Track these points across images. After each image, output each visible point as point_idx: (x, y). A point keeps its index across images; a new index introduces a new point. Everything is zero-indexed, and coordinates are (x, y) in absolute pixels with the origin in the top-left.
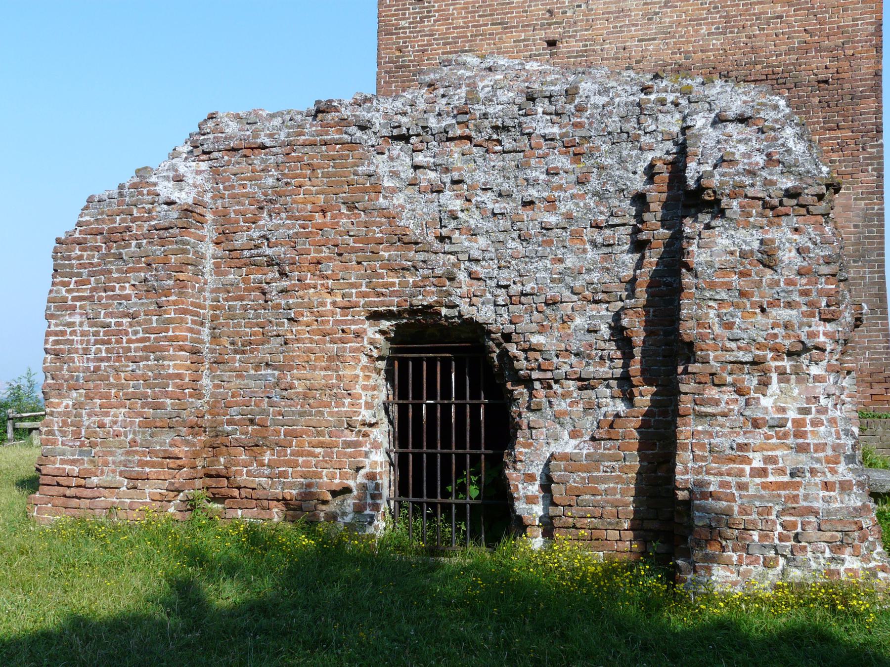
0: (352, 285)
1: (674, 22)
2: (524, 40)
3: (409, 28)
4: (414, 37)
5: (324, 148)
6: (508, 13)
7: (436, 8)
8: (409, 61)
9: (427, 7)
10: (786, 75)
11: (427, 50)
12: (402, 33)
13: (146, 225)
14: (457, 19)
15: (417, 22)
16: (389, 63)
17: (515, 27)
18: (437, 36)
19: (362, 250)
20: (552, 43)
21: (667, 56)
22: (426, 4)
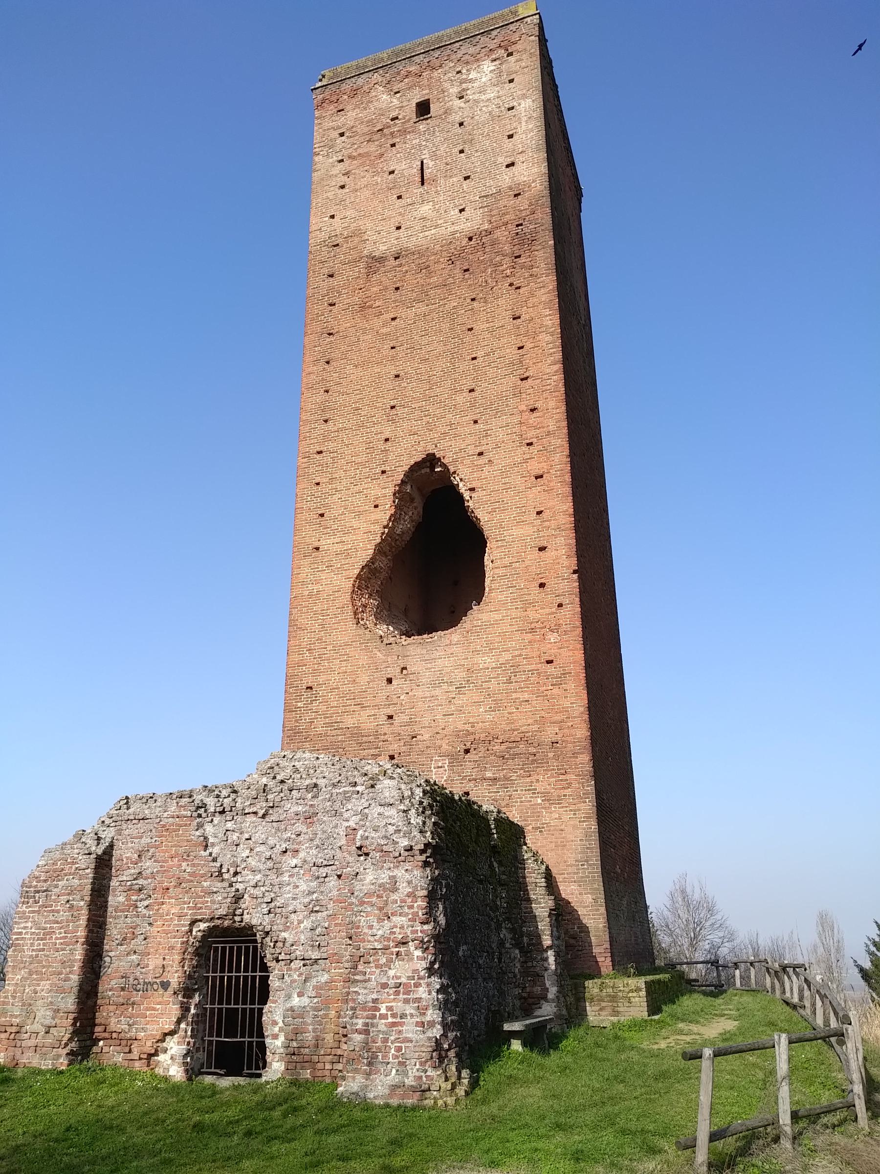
0: (185, 903)
1: (464, 703)
2: (374, 715)
3: (304, 707)
5: (177, 819)
6: (364, 698)
9: (314, 694)
10: (533, 738)
13: (74, 867)
14: (333, 701)
17: (368, 706)
18: (320, 713)
19: (192, 881)
20: (390, 717)
21: (460, 726)
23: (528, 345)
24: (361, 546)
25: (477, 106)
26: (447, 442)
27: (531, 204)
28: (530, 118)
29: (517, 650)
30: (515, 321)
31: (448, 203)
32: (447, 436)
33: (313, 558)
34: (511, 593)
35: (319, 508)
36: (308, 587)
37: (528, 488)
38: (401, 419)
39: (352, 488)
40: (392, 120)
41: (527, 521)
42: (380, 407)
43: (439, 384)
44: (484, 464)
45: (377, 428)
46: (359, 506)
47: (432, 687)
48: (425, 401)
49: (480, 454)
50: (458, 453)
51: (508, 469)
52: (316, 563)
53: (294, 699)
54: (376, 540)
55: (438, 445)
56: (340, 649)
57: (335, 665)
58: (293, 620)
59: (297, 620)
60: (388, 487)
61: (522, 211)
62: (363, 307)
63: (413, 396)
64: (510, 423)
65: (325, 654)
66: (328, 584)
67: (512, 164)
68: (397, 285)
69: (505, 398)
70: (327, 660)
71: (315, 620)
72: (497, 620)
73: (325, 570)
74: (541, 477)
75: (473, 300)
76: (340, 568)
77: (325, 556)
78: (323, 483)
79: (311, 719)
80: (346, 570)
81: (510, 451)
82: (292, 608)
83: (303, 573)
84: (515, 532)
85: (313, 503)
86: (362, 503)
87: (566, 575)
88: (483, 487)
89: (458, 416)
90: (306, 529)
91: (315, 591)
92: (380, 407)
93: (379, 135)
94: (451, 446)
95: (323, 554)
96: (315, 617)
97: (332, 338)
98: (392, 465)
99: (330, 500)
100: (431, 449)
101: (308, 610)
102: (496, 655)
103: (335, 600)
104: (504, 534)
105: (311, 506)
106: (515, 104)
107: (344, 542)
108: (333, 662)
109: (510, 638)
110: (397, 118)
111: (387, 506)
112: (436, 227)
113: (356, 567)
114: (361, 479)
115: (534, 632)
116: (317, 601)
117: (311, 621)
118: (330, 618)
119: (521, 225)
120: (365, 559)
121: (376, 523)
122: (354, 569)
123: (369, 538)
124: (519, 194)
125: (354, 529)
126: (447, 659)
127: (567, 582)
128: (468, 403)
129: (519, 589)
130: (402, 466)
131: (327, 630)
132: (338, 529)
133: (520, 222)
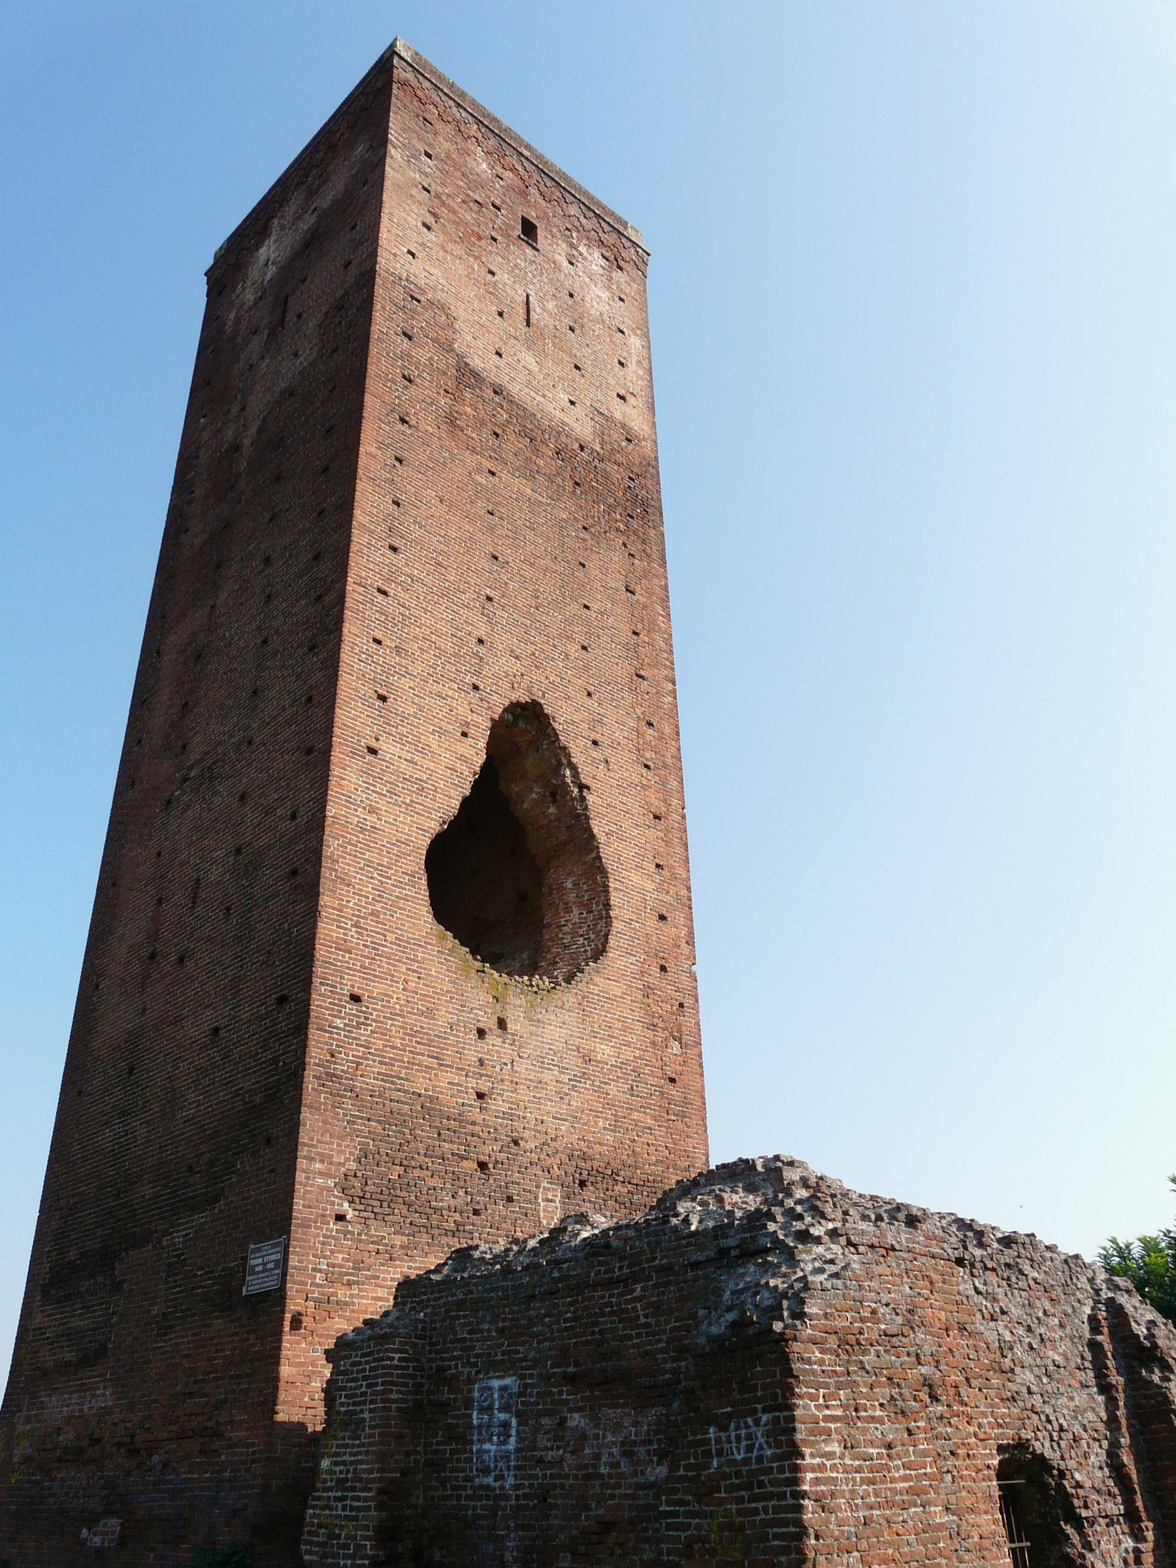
3: (344, 1030)
4: (349, 1044)
7: (374, 1017)
8: (342, 1071)
11: (361, 1064)
12: (336, 1033)
14: (395, 1037)
15: (353, 1026)
16: (318, 1065)
20: (480, 1096)
22: (364, 1009)
47: (540, 1067)
53: (327, 1009)
72: (616, 996)
79: (358, 1057)
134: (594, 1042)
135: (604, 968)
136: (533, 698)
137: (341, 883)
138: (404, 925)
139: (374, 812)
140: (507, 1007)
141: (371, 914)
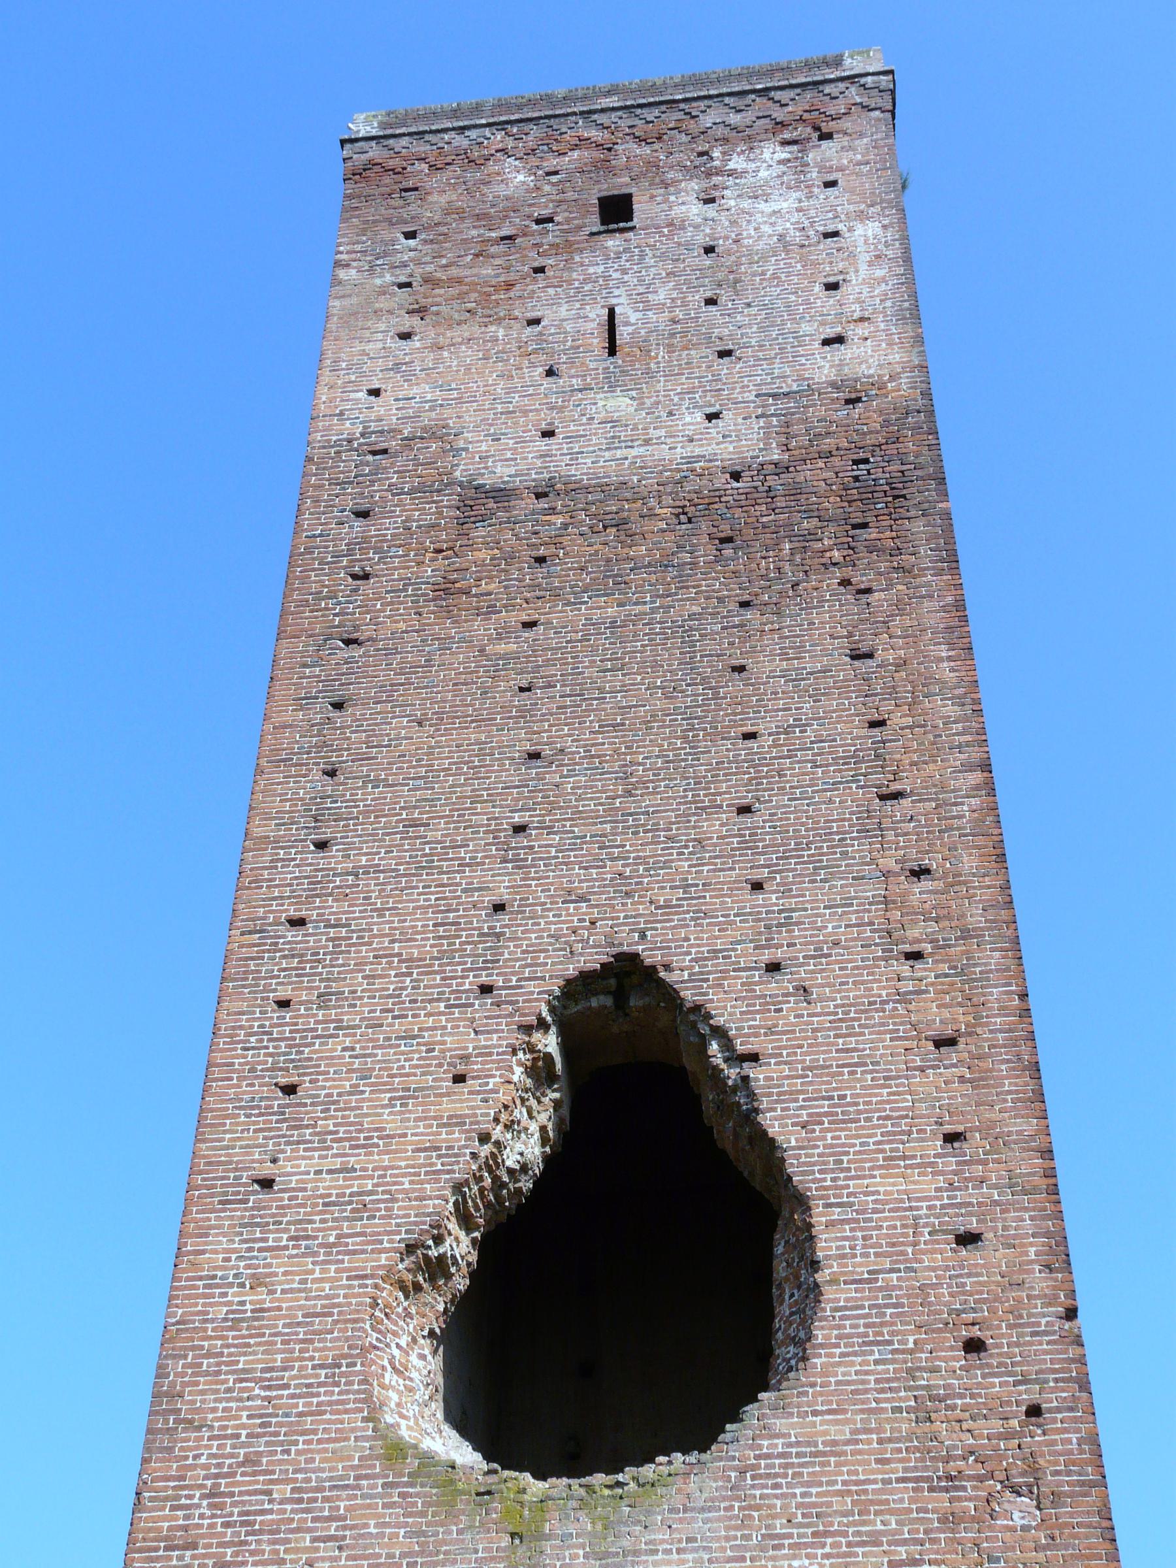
23: (898, 720)
24: (407, 1186)
25: (749, 221)
26: (674, 927)
27: (886, 423)
28: (878, 257)
29: (904, 1542)
30: (857, 663)
31: (676, 399)
32: (676, 913)
33: (252, 1209)
34: (876, 1362)
35: (281, 1069)
36: (225, 1295)
37: (915, 1069)
38: (541, 859)
39: (390, 1025)
40: (539, 221)
41: (914, 1157)
42: (482, 826)
43: (651, 785)
44: (784, 995)
45: (475, 876)
46: (407, 1075)
48: (610, 822)
49: (774, 967)
50: (706, 959)
51: (852, 1015)
52: (258, 1225)
54: (453, 1172)
55: (648, 933)
56: (315, 1500)
57: (297, 1550)
58: (166, 1394)
59: (181, 1396)
60: (496, 1031)
61: (864, 434)
62: (446, 590)
63: (577, 807)
64: (856, 898)
65: (263, 1512)
66: (291, 1291)
67: (840, 340)
68: (542, 552)
69: (837, 838)
70: (271, 1532)
71: (240, 1400)
72: (834, 1443)
73: (286, 1248)
74: (951, 1042)
75: (745, 605)
76: (334, 1245)
77: (289, 1206)
78: (301, 1003)
80: (354, 1252)
81: (857, 968)
82: (166, 1357)
83: (216, 1252)
84: (880, 1184)
85: (266, 1055)
86: (417, 1066)
87: (1043, 1321)
88: (781, 1055)
89: (706, 868)
90: (238, 1124)
91: (248, 1307)
92: (482, 826)
93: (502, 248)
94: (687, 939)
95: (282, 1199)
96: (242, 1390)
97: (356, 652)
98: (513, 974)
99: (316, 1052)
100: (629, 943)
101: (218, 1364)
102: (838, 1556)
103: (311, 1341)
104: (848, 1187)
105: (259, 1063)
106: (840, 227)
107: (355, 1170)
108: (288, 1541)
109: (880, 1502)
110: (550, 220)
111: (491, 1080)
112: (647, 442)
113: (386, 1245)
114: (415, 1001)
115: (956, 1488)
116: (252, 1341)
117: (228, 1400)
118: (293, 1396)
119: (866, 461)
120: (416, 1223)
121: (457, 1124)
122: (380, 1251)
123: (432, 1165)
124: (858, 400)
125: (388, 1136)
126: (675, 1556)
127: (1048, 1343)
128: (735, 840)
129: (903, 1352)
130: (543, 978)
131: (277, 1434)
132: (337, 1132)
133: (862, 455)
134: (773, 1558)
135: (800, 1394)
136: (615, 951)
137: (185, 1430)
138: (313, 1460)
139: (259, 1285)
140: (547, 1547)
141: (242, 1464)
